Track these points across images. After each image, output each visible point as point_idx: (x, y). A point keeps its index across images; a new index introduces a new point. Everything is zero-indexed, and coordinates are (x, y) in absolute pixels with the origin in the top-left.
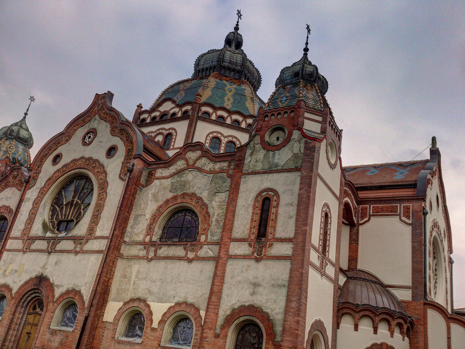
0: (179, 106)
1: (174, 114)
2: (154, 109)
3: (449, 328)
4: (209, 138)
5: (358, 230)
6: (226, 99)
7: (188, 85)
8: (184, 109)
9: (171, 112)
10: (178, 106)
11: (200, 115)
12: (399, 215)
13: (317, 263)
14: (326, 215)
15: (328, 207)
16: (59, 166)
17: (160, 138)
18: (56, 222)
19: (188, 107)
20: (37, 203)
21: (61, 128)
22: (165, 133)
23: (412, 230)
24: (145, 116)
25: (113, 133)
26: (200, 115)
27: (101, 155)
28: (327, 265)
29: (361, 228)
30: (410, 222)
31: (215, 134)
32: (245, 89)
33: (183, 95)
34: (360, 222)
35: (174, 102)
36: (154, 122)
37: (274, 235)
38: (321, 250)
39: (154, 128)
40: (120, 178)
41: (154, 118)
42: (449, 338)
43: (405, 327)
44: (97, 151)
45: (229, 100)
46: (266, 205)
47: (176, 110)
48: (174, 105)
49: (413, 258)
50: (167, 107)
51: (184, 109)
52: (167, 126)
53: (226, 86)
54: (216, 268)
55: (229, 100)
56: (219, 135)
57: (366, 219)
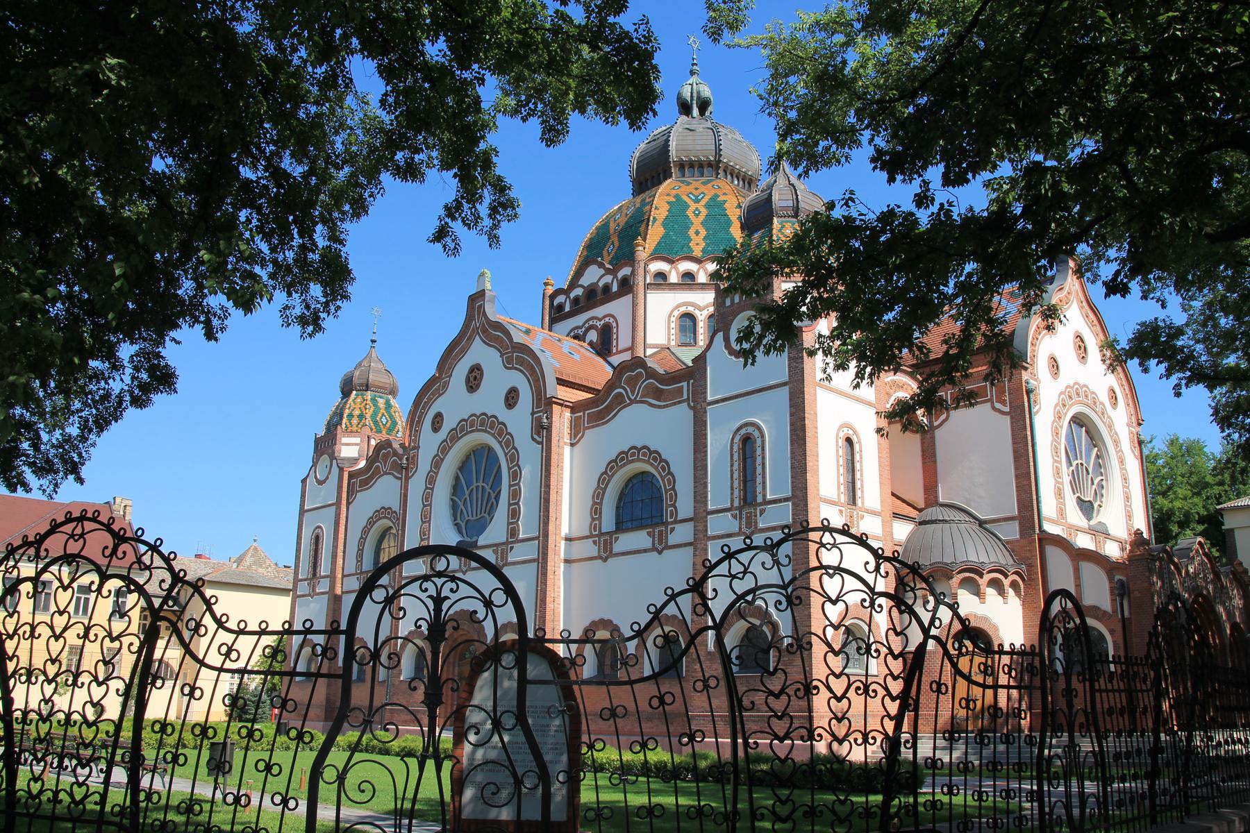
0: (613, 272)
1: (607, 288)
2: (573, 284)
4: (673, 319)
5: (933, 439)
6: (691, 233)
7: (622, 220)
8: (620, 275)
9: (601, 284)
10: (608, 271)
11: (648, 281)
14: (849, 441)
15: (850, 427)
16: (443, 433)
17: (593, 336)
18: (463, 525)
19: (626, 271)
20: (427, 498)
21: (431, 371)
22: (599, 324)
23: (1012, 423)
24: (560, 299)
25: (509, 364)
26: (648, 281)
28: (862, 517)
29: (938, 433)
30: (1007, 409)
31: (683, 309)
32: (725, 202)
33: (617, 244)
34: (936, 424)
35: (601, 265)
36: (579, 306)
37: (764, 496)
39: (579, 320)
40: (534, 439)
41: (576, 300)
43: (1006, 582)
44: (489, 399)
45: (697, 233)
46: (747, 446)
47: (608, 279)
48: (602, 271)
49: (1016, 469)
50: (593, 275)
51: (620, 275)
52: (599, 311)
54: (695, 555)
55: (697, 233)
56: (690, 309)
57: (944, 416)
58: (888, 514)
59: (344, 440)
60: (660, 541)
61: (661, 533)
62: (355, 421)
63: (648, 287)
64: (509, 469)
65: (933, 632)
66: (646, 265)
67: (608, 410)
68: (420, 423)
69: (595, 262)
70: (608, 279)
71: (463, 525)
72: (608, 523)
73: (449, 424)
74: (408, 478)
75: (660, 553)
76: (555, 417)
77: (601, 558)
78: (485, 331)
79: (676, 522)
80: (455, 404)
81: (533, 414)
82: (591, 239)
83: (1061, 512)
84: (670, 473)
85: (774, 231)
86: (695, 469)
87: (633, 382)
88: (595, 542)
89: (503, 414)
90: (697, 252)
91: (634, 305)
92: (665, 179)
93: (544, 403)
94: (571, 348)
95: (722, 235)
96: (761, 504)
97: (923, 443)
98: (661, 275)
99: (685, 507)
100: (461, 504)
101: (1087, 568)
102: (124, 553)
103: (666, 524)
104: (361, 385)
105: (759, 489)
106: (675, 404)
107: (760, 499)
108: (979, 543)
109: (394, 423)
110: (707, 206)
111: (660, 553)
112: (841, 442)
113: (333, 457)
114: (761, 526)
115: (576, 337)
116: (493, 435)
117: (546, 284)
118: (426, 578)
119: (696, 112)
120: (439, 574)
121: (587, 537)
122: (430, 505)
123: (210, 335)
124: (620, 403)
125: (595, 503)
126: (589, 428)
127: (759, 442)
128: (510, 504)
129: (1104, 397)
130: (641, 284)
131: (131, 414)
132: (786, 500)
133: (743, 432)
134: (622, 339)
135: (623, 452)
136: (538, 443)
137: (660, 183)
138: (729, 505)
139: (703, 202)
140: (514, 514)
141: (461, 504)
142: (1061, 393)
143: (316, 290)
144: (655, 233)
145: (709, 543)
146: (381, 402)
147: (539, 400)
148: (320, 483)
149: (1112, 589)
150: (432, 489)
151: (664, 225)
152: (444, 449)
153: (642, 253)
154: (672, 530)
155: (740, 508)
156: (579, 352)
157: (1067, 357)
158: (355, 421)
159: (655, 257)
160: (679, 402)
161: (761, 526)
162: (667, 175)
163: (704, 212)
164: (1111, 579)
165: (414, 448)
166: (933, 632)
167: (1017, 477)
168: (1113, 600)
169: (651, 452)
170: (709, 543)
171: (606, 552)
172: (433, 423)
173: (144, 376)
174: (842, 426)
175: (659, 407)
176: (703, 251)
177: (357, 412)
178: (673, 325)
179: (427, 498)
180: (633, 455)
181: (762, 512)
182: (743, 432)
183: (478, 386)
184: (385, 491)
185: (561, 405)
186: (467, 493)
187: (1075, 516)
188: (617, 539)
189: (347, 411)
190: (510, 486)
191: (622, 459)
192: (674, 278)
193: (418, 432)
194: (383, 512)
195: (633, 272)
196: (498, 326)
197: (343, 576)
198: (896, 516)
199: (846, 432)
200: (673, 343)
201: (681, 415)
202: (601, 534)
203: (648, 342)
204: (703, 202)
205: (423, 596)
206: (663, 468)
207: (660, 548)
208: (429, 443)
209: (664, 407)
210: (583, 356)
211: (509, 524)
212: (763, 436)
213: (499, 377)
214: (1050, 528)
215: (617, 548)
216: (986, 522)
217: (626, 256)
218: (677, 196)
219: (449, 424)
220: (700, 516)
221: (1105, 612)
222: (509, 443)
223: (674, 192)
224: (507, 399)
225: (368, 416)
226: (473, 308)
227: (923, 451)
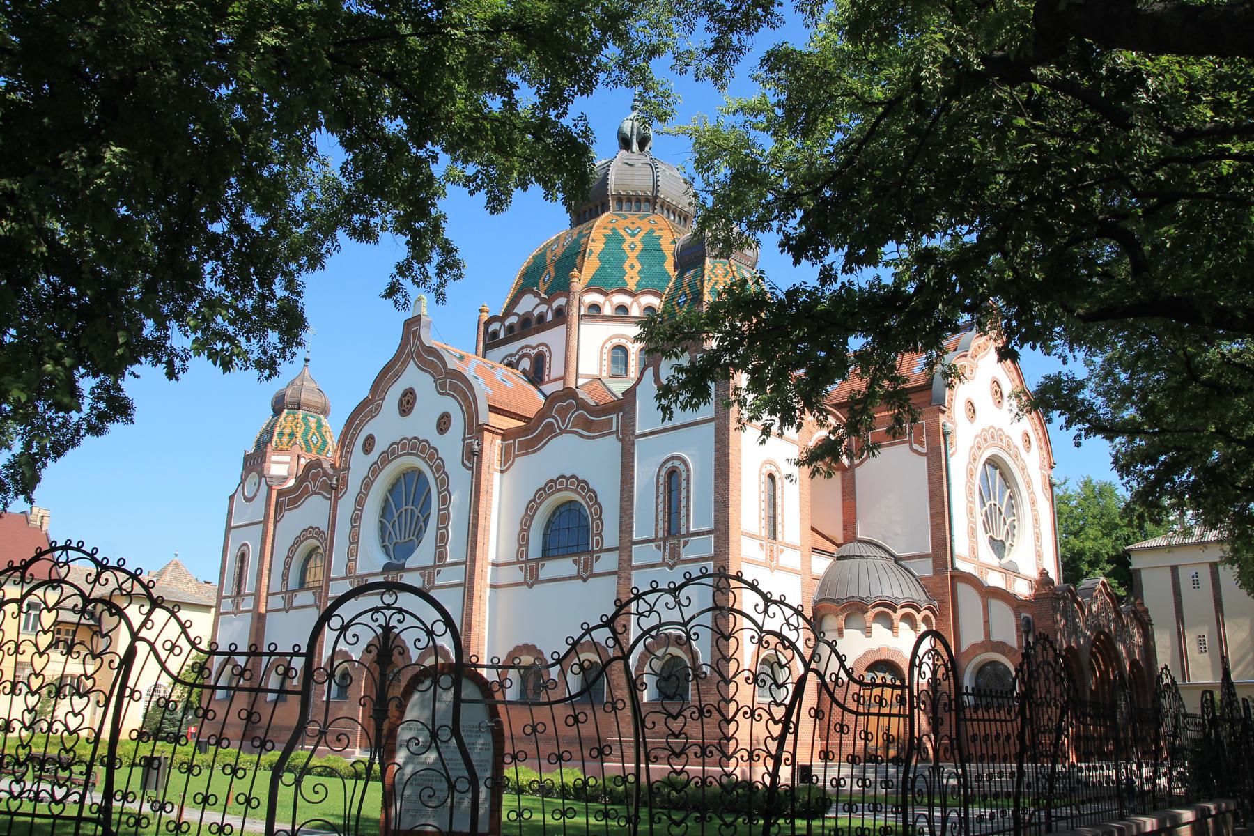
1: (541, 317)
2: (508, 312)
3: (986, 608)
4: (605, 350)
5: (853, 476)
6: (626, 266)
7: (559, 251)
9: (536, 313)
10: (543, 301)
12: (909, 441)
13: (761, 555)
14: (771, 477)
16: (374, 456)
17: (526, 364)
18: (391, 547)
19: (561, 301)
20: (356, 519)
21: (365, 393)
22: (533, 353)
24: (495, 326)
25: (442, 389)
27: (427, 430)
28: (782, 551)
30: (924, 450)
31: (615, 341)
35: (537, 295)
36: (514, 334)
37: (688, 528)
38: (764, 533)
39: (513, 347)
40: (464, 465)
41: (511, 329)
42: (987, 622)
43: (919, 617)
44: (421, 424)
45: (632, 267)
46: (673, 478)
47: (543, 308)
48: (537, 301)
49: (931, 508)
50: (528, 304)
52: (533, 340)
53: (624, 240)
55: (632, 267)
58: (808, 548)
59: (274, 458)
60: (586, 569)
61: (586, 561)
62: (285, 440)
63: (582, 317)
64: (439, 493)
65: (813, 665)
66: (581, 296)
67: (539, 438)
68: (351, 444)
69: (532, 292)
70: (543, 308)
71: (391, 547)
72: (535, 550)
73: (380, 446)
74: (337, 499)
75: (585, 580)
76: (486, 445)
77: (527, 584)
78: (419, 356)
79: (601, 551)
80: (387, 427)
81: (464, 440)
82: (527, 268)
83: (974, 551)
84: (597, 503)
85: (706, 272)
86: (622, 500)
87: (563, 412)
88: (521, 568)
89: (435, 439)
90: (631, 286)
91: (568, 335)
92: (603, 212)
93: (476, 430)
94: (504, 375)
95: (656, 269)
96: (684, 536)
97: (843, 481)
98: (595, 307)
99: (611, 536)
100: (389, 526)
101: (996, 605)
102: (107, 580)
103: (592, 552)
104: (293, 403)
105: (683, 521)
106: (604, 435)
107: (683, 531)
108: (894, 580)
109: (325, 443)
110: (643, 241)
111: (585, 580)
112: (764, 478)
113: (261, 475)
114: (683, 557)
115: (509, 365)
116: (424, 459)
117: (482, 311)
118: (377, 610)
119: (635, 147)
120: (389, 607)
121: (514, 563)
122: (359, 527)
123: (171, 374)
124: (550, 432)
125: (522, 530)
126: (519, 456)
127: (684, 475)
128: (438, 529)
129: (1018, 441)
130: (575, 314)
131: (88, 441)
132: (709, 532)
133: (669, 465)
134: (555, 368)
135: (551, 481)
136: (469, 469)
137: (598, 216)
138: (653, 536)
139: (639, 237)
140: (442, 538)
141: (389, 526)
142: (977, 436)
143: (273, 337)
144: (591, 265)
145: (633, 573)
146: (313, 421)
147: (471, 426)
148: (248, 500)
149: (1018, 626)
150: (361, 511)
151: (600, 258)
152: (375, 471)
153: (577, 285)
154: (598, 558)
155: (664, 540)
156: (511, 379)
157: (984, 401)
158: (285, 440)
159: (590, 288)
160: (609, 434)
161: (683, 557)
162: (605, 208)
163: (640, 246)
164: (1017, 616)
165: (344, 469)
166: (813, 665)
167: (932, 516)
168: (1019, 637)
169: (579, 482)
170: (633, 573)
171: (532, 579)
172: (364, 445)
173: (102, 406)
174: (765, 463)
175: (589, 438)
176: (638, 285)
177: (288, 431)
178: (605, 356)
179: (356, 519)
180: (562, 483)
181: (685, 544)
182: (669, 465)
183: (410, 410)
184: (313, 510)
185: (493, 432)
186: (396, 515)
187: (987, 554)
188: (543, 566)
189: (278, 430)
190: (439, 510)
191: (551, 488)
192: (607, 310)
193: (349, 453)
194: (311, 532)
195: (568, 303)
196: (433, 352)
197: (268, 594)
198: (816, 550)
199: (769, 468)
200: (604, 374)
201: (609, 446)
202: (528, 561)
203: (580, 372)
204: (639, 237)
205: (374, 625)
206: (590, 498)
207: (585, 576)
208: (360, 464)
209: (593, 438)
210: (515, 384)
211: (437, 547)
212: (688, 470)
213: (431, 403)
214: (962, 566)
215: (543, 574)
216: (901, 558)
217: (562, 287)
218: (614, 230)
219: (380, 446)
220: (625, 546)
221: (1012, 648)
222: (439, 468)
223: (611, 226)
224: (439, 424)
225: (299, 435)
226: (409, 333)
227: (843, 488)
